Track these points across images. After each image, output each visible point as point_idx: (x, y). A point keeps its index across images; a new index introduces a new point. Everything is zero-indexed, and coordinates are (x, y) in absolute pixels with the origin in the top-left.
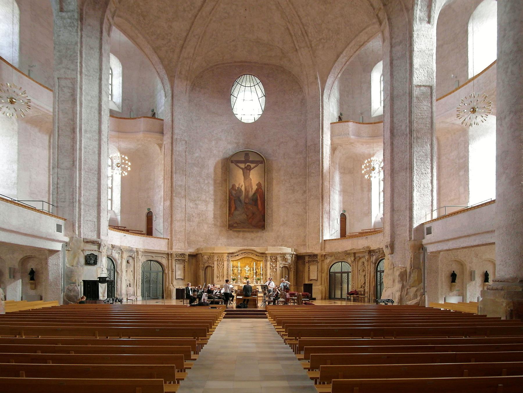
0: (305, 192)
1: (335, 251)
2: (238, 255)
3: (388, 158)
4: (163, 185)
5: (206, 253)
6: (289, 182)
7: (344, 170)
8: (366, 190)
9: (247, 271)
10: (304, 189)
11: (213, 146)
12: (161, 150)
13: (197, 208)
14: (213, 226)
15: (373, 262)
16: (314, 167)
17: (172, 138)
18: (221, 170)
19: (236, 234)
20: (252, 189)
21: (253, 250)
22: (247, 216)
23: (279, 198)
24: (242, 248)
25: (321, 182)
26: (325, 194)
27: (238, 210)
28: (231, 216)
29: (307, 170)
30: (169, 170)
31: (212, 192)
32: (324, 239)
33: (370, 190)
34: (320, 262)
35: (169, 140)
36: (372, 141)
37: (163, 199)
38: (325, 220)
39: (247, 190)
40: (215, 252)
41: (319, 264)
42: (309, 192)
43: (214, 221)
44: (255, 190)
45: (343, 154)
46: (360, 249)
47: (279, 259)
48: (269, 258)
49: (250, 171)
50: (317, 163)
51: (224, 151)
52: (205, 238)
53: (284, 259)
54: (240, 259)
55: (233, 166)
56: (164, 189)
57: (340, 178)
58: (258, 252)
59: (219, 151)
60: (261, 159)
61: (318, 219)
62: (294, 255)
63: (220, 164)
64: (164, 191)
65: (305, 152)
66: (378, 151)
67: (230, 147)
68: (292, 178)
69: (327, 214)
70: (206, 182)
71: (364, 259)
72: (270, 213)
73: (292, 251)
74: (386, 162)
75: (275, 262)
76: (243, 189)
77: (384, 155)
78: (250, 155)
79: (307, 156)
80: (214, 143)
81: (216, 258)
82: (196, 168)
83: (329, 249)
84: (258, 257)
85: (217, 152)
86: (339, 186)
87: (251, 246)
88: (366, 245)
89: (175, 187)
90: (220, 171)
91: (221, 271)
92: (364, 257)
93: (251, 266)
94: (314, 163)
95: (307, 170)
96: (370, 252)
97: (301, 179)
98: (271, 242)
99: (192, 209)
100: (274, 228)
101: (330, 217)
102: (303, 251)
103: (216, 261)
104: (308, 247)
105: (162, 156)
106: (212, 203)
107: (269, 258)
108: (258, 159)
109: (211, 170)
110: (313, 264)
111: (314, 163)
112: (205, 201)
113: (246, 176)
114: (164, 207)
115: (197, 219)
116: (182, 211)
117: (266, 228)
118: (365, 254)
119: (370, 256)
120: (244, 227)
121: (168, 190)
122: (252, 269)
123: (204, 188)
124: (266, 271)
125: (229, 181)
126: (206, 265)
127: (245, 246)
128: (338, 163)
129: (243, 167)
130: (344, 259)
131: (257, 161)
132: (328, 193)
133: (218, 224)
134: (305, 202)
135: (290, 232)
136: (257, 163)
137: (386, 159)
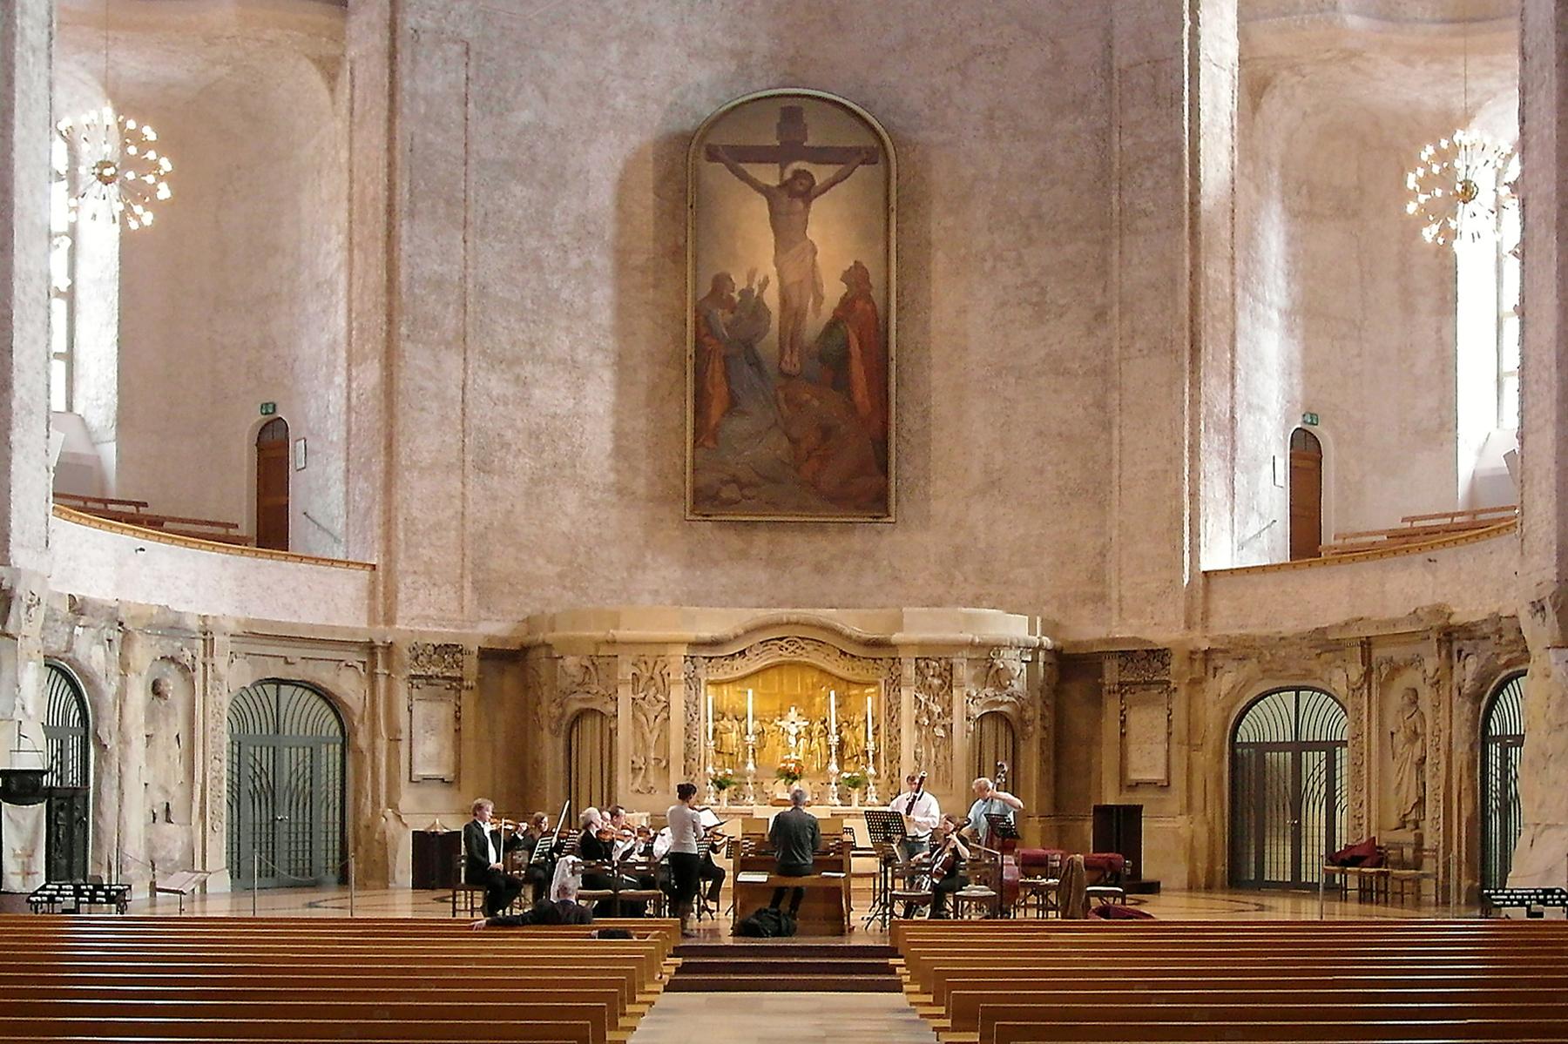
0: (1101, 315)
1: (1265, 631)
2: (742, 653)
3: (1547, 132)
4: (342, 279)
5: (572, 645)
6: (1020, 265)
7: (1310, 195)
8: (1425, 304)
9: (792, 740)
10: (1098, 301)
11: (609, 72)
12: (332, 90)
13: (524, 401)
14: (613, 498)
15: (1466, 690)
16: (1149, 184)
17: (393, 27)
18: (651, 195)
19: (734, 541)
20: (819, 298)
21: (824, 628)
22: (792, 441)
23: (966, 349)
24: (764, 614)
25: (1187, 262)
26: (1210, 330)
27: (743, 413)
28: (710, 444)
29: (1115, 198)
30: (374, 199)
31: (605, 317)
32: (1205, 566)
33: (1447, 303)
34: (1183, 692)
35: (379, 40)
36: (1458, 42)
37: (344, 354)
38: (1211, 464)
39: (795, 302)
40: (622, 634)
41: (1179, 702)
42: (1121, 314)
43: (618, 471)
44: (836, 304)
45: (1305, 113)
46: (1394, 623)
47: (963, 672)
48: (909, 671)
49: (807, 204)
50: (1168, 159)
51: (669, 99)
52: (570, 563)
53: (993, 675)
54: (757, 673)
55: (716, 175)
56: (350, 301)
57: (1291, 240)
58: (849, 638)
59: (644, 96)
60: (863, 140)
61: (1174, 460)
62: (1041, 654)
63: (650, 166)
64: (350, 311)
65: (1102, 101)
66: (1492, 94)
67: (701, 74)
68: (1031, 241)
69: (1218, 432)
70: (575, 262)
71: (1419, 676)
72: (916, 427)
73: (1032, 631)
74: (1534, 155)
76: (772, 298)
77: (1522, 120)
78: (808, 118)
79: (1111, 125)
80: (614, 51)
81: (625, 671)
82: (518, 190)
83: (1227, 621)
85: (632, 103)
86: (1281, 282)
87: (815, 606)
88: (1427, 601)
89: (411, 287)
90: (650, 203)
91: (652, 739)
92: (1415, 662)
94: (1150, 160)
95: (1115, 198)
96: (1449, 634)
97: (1081, 244)
98: (920, 582)
99: (501, 408)
100: (937, 507)
101: (1234, 449)
102: (1088, 630)
103: (626, 683)
104: (1115, 611)
105: (339, 125)
106: (607, 375)
107: (909, 671)
108: (857, 139)
109: (603, 198)
110: (1145, 703)
111: (1150, 160)
112: (569, 364)
113: (786, 230)
114: (349, 399)
115: (526, 462)
116: (444, 418)
117: (893, 514)
118: (1421, 648)
119: (1449, 655)
120: (775, 505)
121: (370, 306)
122: (817, 727)
123: (565, 294)
124: (895, 737)
125: (696, 257)
126: (574, 706)
127: (779, 605)
128: (1276, 160)
129: (773, 182)
130: (1309, 673)
131: (847, 150)
132: (1222, 319)
133: (640, 485)
134: (1104, 372)
135: (1022, 531)
136: (845, 158)
137: (1533, 140)
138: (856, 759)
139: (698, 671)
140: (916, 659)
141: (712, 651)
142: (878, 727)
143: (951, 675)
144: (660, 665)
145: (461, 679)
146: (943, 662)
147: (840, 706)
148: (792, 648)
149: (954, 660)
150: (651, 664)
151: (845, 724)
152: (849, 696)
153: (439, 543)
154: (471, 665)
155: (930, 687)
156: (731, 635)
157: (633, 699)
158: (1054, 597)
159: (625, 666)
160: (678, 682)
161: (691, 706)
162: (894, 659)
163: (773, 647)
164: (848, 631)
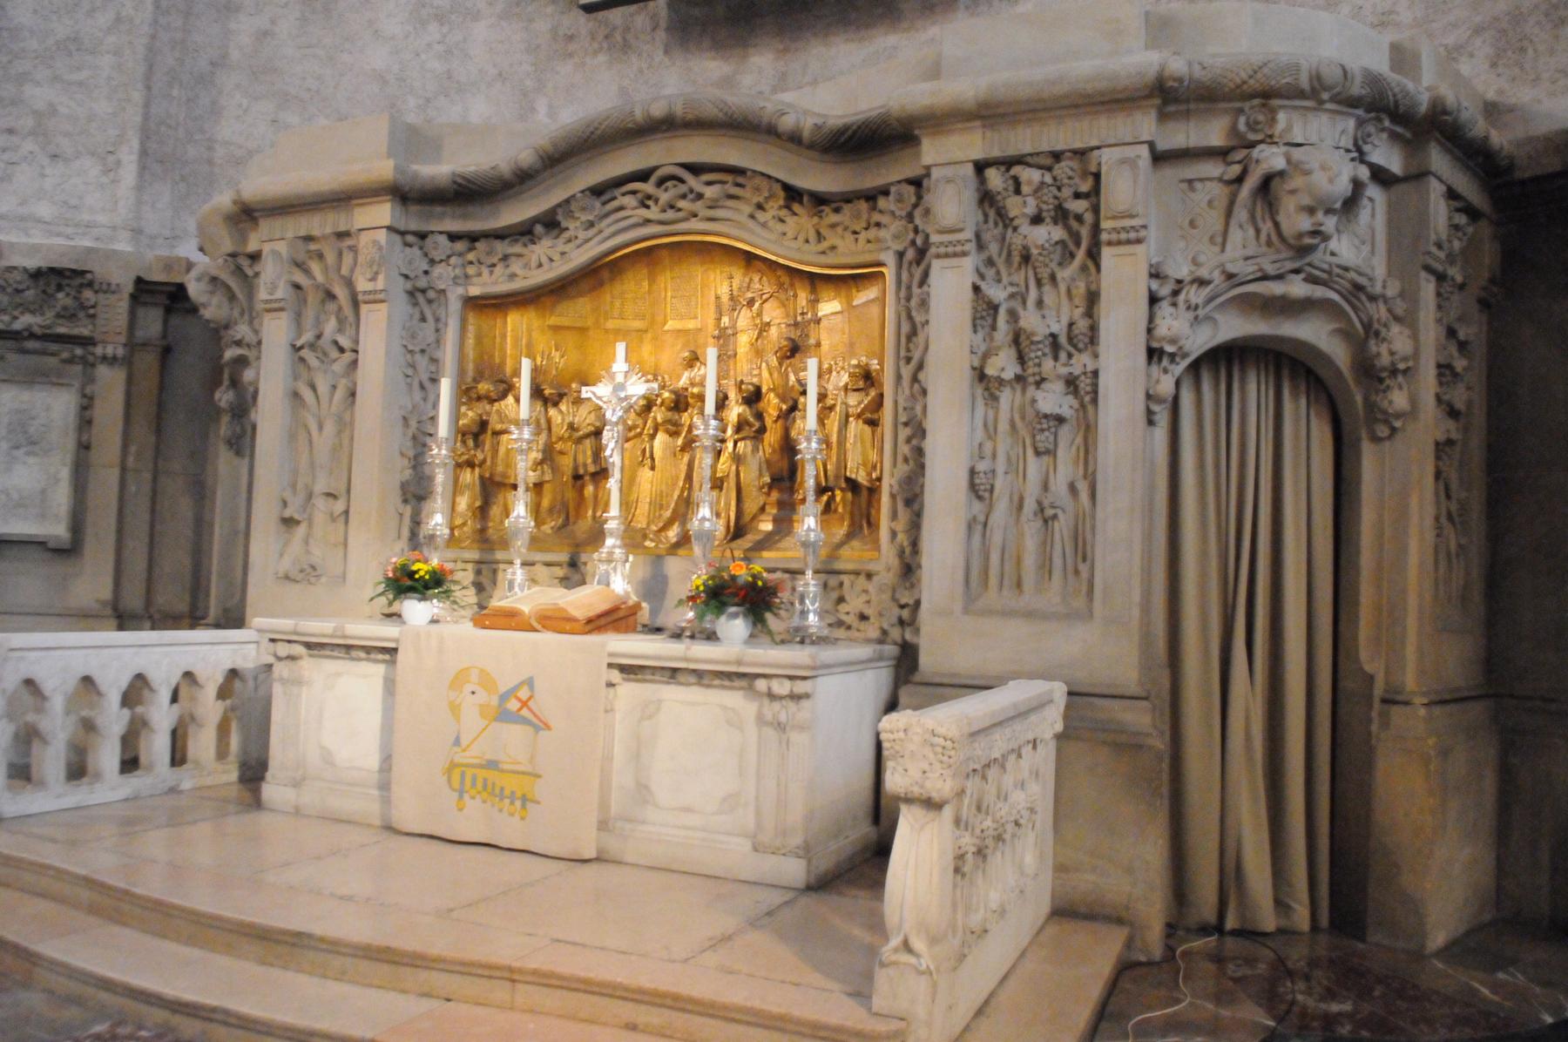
2: (551, 223)
58: (794, 139)
140: (980, 167)
141: (465, 217)
143: (1096, 210)
145: (86, 342)
148: (664, 197)
149: (1107, 157)
152: (818, 321)
153: (75, 77)
154: (115, 313)
155: (1026, 258)
156: (505, 168)
158: (1478, 31)
161: (422, 362)
162: (917, 183)
163: (629, 201)
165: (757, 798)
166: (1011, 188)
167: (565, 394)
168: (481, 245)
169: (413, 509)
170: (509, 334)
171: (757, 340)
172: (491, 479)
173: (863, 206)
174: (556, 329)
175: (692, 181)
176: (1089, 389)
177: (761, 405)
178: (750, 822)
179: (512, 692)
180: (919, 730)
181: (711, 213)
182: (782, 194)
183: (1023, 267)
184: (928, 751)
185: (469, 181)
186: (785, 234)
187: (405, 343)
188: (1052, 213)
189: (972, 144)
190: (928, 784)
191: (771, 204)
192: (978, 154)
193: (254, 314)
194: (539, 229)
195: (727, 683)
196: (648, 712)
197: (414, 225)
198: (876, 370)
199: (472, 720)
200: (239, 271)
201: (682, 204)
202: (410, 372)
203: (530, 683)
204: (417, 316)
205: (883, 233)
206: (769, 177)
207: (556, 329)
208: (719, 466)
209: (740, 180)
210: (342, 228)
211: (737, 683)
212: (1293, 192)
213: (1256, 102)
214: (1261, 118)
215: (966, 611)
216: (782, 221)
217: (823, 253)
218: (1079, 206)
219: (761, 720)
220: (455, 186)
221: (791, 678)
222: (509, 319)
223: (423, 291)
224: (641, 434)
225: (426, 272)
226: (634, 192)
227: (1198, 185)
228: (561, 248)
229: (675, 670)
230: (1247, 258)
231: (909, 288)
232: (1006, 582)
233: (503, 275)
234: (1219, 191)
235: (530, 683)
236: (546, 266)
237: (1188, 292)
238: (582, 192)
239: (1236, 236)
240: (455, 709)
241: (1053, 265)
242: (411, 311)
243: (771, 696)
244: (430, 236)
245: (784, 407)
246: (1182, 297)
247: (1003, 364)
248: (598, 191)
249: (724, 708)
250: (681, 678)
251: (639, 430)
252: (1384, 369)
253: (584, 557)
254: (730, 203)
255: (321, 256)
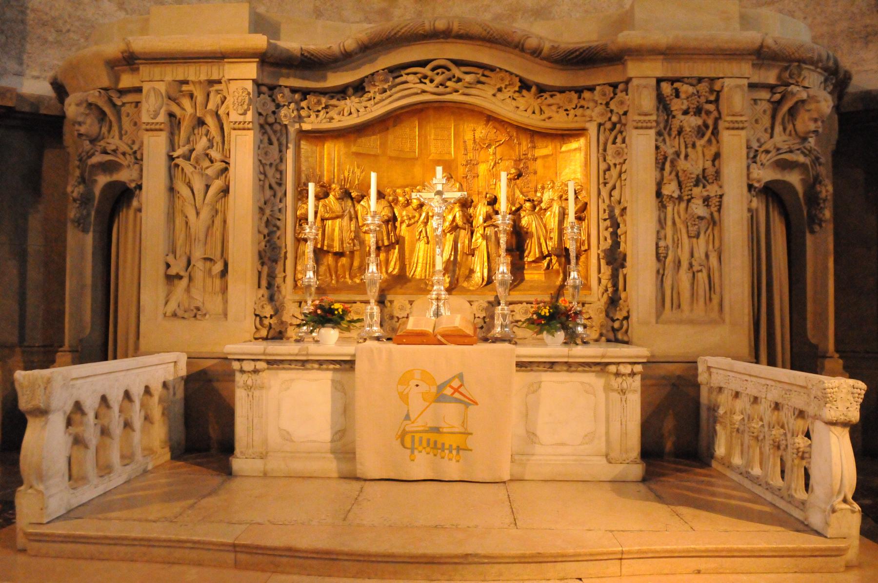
2: (359, 88)
58: (536, 53)
75: (700, 132)
84: (535, 104)
91: (198, 225)
93: (480, 184)
103: (153, 129)
107: (648, 101)
138: (545, 263)
139: (283, 112)
140: (659, 81)
141: (304, 78)
142: (584, 207)
144: (214, 100)
146: (703, 87)
147: (519, 175)
148: (438, 79)
150: (200, 97)
151: (528, 205)
152: (535, 159)
157: (171, 158)
159: (152, 99)
160: (240, 127)
161: (271, 172)
162: (615, 86)
163: (411, 78)
164: (532, 43)
165: (607, 433)
166: (674, 94)
167: (365, 196)
168: (312, 99)
169: (269, 268)
170: (325, 156)
171: (493, 168)
172: (321, 249)
173: (574, 96)
174: (357, 154)
175: (457, 72)
176: (717, 204)
177: (497, 206)
178: (602, 446)
179: (447, 383)
180: (845, 386)
181: (467, 91)
182: (519, 84)
183: (677, 137)
184: (850, 397)
185: (312, 55)
186: (518, 108)
187: (261, 158)
188: (695, 110)
189: (656, 68)
190: (850, 414)
191: (508, 89)
192: (659, 74)
193: (123, 132)
194: (350, 91)
195: (587, 369)
196: (535, 388)
197: (267, 81)
198: (579, 189)
199: (416, 404)
200: (110, 100)
201: (448, 83)
202: (262, 177)
203: (460, 377)
204: (266, 140)
205: (588, 112)
206: (511, 74)
207: (357, 154)
208: (473, 240)
209: (487, 73)
210: (215, 77)
211: (593, 369)
212: (809, 111)
213: (796, 64)
214: (796, 72)
215: (657, 323)
216: (513, 99)
217: (544, 120)
218: (711, 107)
219: (607, 388)
220: (303, 58)
221: (630, 363)
222: (325, 147)
223: (271, 125)
224: (417, 222)
225: (274, 113)
226: (415, 74)
227: (759, 102)
228: (364, 104)
229: (553, 363)
230: (784, 141)
231: (605, 144)
232: (674, 306)
233: (325, 118)
234: (765, 106)
235: (460, 377)
236: (355, 115)
237: (760, 157)
238: (383, 70)
239: (778, 129)
240: (404, 398)
241: (694, 137)
242: (262, 138)
243: (617, 374)
244: (278, 89)
245: (514, 209)
246: (758, 158)
247: (672, 188)
248: (395, 71)
249: (582, 383)
250: (557, 368)
251: (416, 219)
252: (821, 199)
253: (389, 297)
254: (479, 86)
255: (191, 96)
